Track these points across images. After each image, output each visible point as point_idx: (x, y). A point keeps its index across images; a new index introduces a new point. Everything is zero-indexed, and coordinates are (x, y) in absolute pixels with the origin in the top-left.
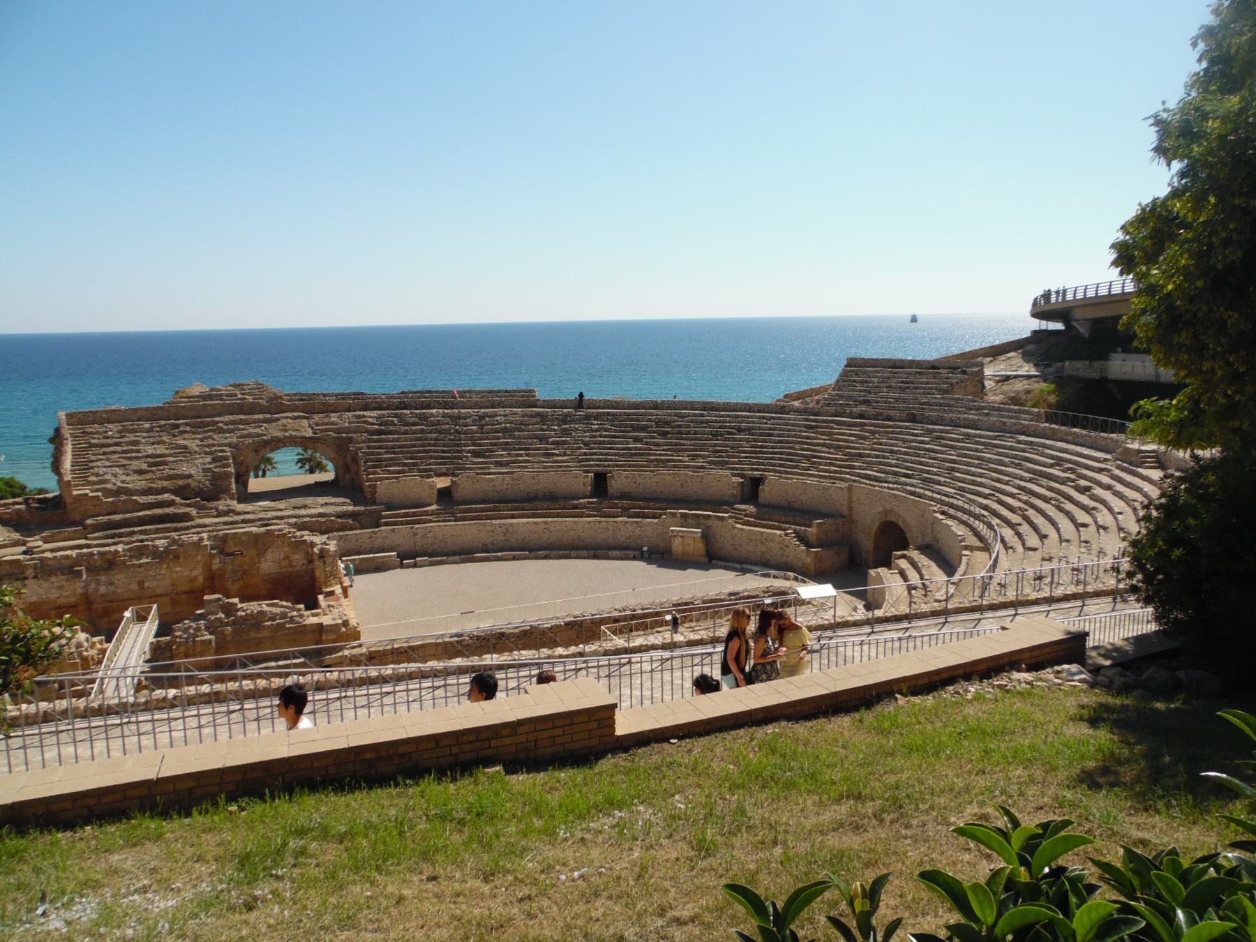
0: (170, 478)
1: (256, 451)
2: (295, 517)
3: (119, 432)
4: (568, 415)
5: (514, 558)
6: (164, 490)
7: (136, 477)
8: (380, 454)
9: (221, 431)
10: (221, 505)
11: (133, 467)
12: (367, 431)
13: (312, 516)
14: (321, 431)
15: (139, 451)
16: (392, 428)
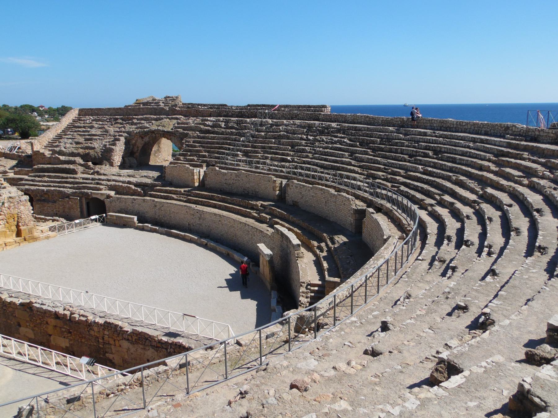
0: (87, 148)
1: (142, 138)
2: (116, 181)
3: (93, 120)
4: (328, 127)
5: (190, 241)
6: (78, 155)
7: (74, 145)
8: (195, 147)
9: (133, 124)
10: (97, 168)
11: (76, 140)
12: (201, 131)
13: (123, 182)
14: (176, 128)
15: (89, 132)
16: (216, 129)
